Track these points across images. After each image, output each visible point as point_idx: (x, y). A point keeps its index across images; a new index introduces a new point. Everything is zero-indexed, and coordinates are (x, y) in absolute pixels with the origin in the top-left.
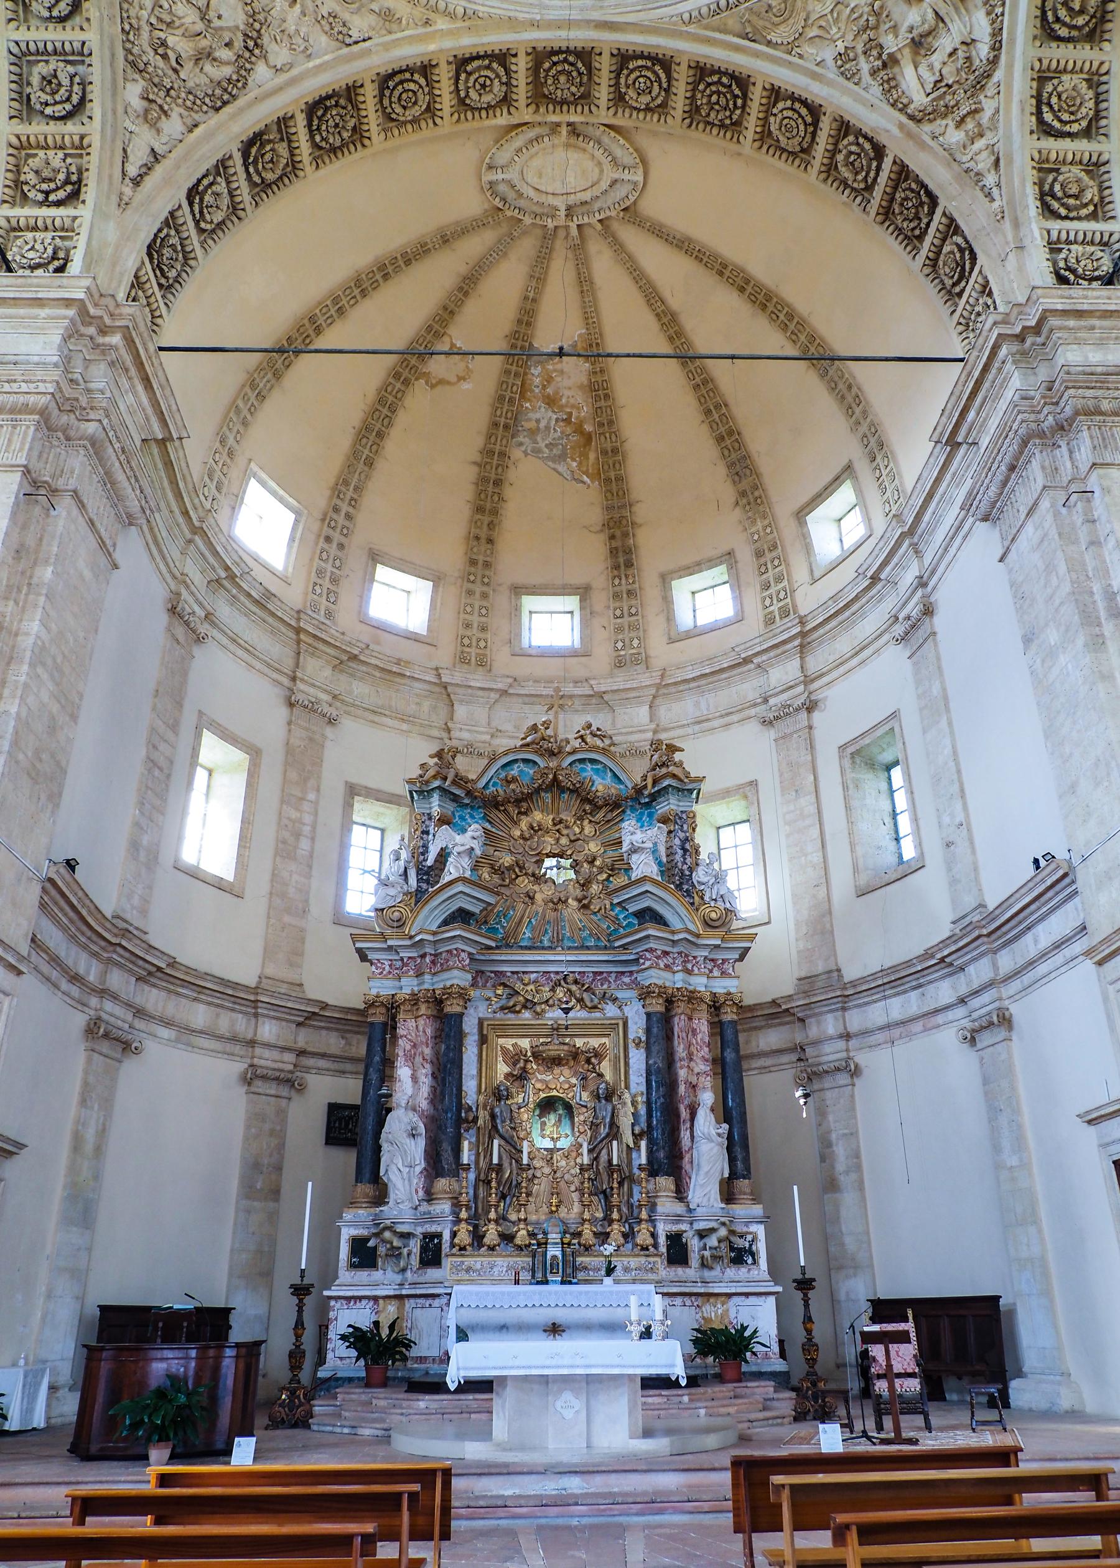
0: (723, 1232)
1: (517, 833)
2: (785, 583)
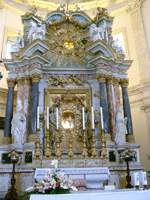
0: (127, 151)
1: (57, 35)
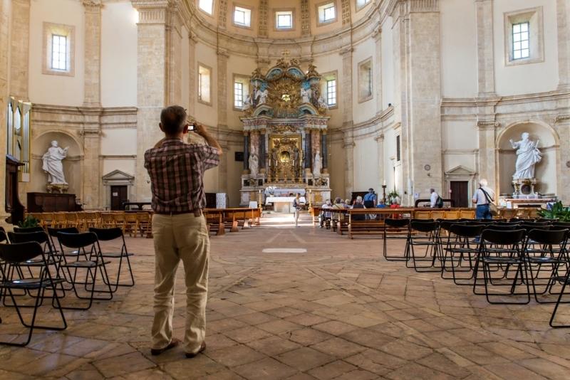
2: (349, 12)
